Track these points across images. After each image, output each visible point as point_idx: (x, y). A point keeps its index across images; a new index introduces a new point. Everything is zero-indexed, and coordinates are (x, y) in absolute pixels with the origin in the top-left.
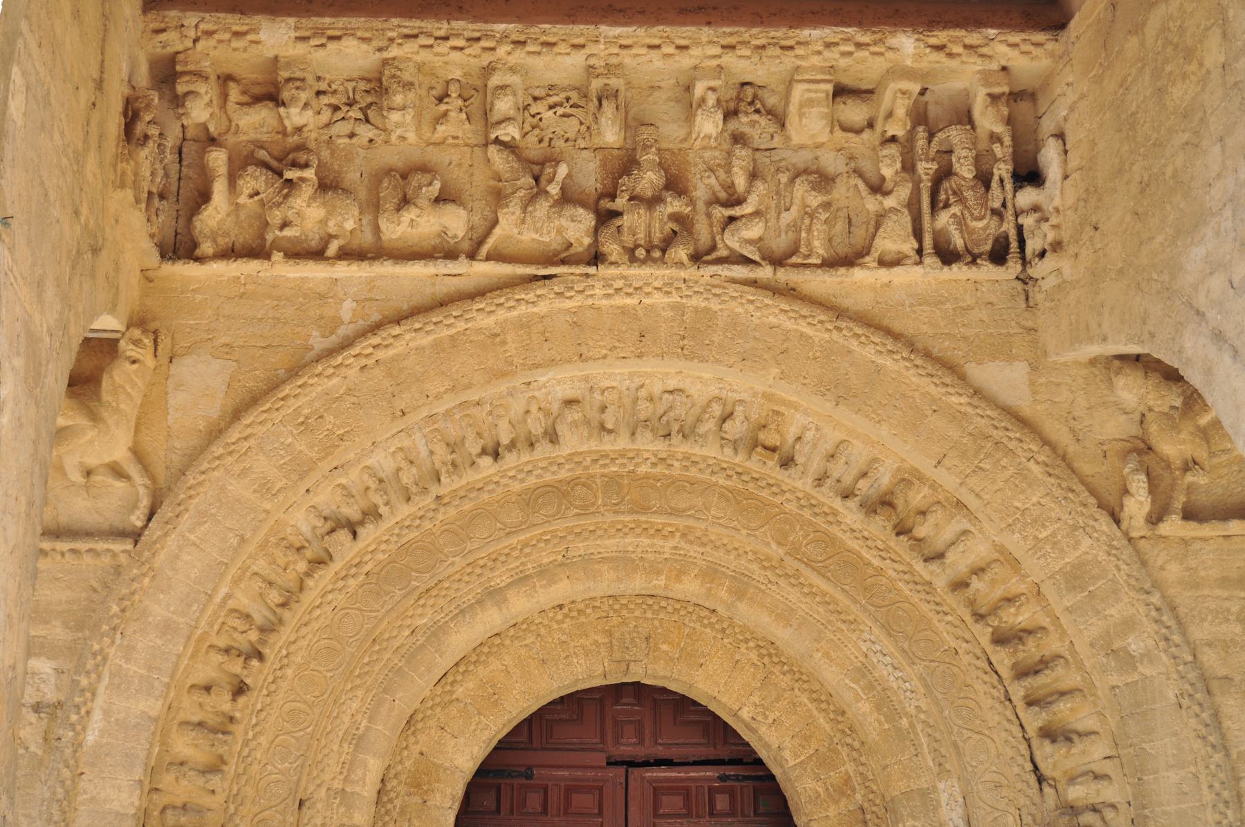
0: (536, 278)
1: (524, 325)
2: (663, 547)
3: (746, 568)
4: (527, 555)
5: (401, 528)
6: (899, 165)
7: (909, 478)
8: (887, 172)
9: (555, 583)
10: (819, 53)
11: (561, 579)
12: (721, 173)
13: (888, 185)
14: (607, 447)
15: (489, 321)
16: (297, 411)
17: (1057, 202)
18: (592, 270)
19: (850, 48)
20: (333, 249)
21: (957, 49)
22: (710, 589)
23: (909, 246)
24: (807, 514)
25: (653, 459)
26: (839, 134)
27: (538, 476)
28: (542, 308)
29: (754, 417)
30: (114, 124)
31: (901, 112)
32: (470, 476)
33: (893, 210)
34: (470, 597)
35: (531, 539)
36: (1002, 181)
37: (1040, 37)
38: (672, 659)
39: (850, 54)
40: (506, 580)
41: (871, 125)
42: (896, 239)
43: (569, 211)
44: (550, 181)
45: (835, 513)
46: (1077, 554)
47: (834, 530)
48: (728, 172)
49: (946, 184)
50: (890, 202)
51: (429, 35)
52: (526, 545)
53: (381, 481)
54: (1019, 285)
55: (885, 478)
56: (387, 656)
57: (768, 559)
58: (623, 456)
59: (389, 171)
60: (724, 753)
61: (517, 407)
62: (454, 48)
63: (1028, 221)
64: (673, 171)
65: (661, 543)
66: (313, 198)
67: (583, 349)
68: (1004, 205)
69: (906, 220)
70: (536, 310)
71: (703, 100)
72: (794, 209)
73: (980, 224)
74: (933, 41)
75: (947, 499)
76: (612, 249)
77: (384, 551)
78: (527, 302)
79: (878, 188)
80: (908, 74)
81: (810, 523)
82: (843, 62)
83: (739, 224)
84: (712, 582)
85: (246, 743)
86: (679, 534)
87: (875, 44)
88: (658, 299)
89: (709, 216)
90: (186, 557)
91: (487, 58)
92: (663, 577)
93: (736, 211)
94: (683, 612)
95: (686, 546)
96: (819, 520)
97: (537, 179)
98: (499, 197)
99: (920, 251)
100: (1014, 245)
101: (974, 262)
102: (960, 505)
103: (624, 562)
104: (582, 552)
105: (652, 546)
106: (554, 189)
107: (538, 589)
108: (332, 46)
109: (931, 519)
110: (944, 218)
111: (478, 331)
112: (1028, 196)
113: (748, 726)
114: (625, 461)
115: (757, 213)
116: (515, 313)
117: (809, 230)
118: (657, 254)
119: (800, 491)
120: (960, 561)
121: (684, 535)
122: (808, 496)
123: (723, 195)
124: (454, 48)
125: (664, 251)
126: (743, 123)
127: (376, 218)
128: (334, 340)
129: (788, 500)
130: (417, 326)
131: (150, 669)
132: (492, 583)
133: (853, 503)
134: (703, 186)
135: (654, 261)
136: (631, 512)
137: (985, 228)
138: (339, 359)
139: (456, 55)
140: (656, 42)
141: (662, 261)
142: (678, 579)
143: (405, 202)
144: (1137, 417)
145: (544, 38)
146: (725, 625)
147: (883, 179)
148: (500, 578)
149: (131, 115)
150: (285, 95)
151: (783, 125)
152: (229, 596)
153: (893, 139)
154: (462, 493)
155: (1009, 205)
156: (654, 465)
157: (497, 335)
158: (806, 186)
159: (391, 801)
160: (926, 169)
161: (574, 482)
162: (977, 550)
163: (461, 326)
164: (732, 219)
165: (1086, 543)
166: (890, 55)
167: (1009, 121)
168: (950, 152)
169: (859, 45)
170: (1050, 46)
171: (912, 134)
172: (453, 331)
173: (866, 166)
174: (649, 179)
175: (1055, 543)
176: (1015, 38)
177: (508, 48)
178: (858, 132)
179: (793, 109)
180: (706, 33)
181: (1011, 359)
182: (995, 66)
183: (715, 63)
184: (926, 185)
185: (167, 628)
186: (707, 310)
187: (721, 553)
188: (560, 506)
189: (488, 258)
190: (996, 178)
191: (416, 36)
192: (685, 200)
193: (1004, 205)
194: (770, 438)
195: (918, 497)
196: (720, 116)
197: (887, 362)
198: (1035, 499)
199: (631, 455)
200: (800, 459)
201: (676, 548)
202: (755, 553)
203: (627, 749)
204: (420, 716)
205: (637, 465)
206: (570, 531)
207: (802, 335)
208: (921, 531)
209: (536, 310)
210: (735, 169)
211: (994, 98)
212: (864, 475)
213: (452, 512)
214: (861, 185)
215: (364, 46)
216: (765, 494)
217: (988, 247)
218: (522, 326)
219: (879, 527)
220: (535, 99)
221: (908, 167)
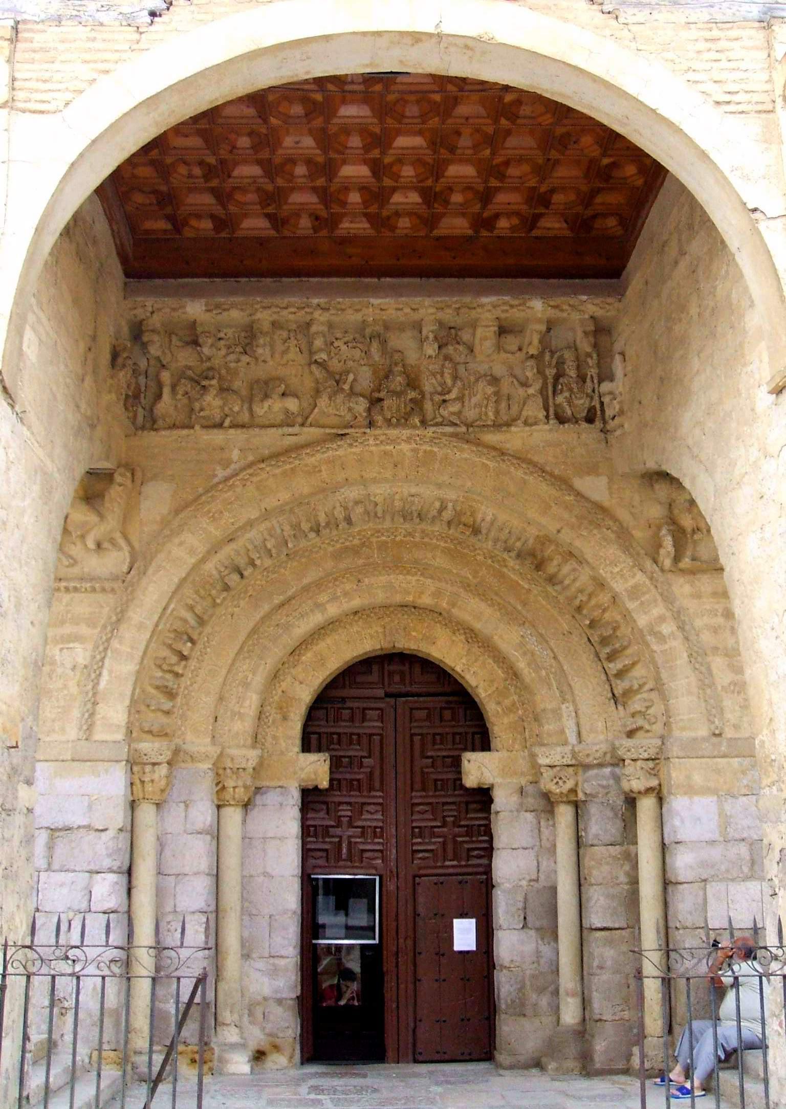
0: (339, 435)
1: (330, 462)
5: (268, 572)
6: (535, 370)
7: (544, 540)
8: (529, 374)
10: (489, 311)
12: (438, 376)
13: (530, 382)
16: (209, 512)
17: (621, 389)
18: (368, 431)
19: (505, 308)
20: (227, 423)
21: (565, 307)
23: (541, 414)
29: (458, 508)
30: (106, 357)
31: (536, 341)
33: (534, 395)
36: (592, 377)
37: (610, 300)
39: (507, 311)
41: (520, 349)
42: (534, 410)
43: (353, 399)
44: (344, 383)
45: (504, 560)
47: (505, 570)
48: (442, 376)
49: (561, 380)
50: (531, 391)
51: (277, 306)
53: (255, 547)
54: (603, 435)
59: (257, 381)
60: (448, 689)
62: (291, 313)
63: (606, 400)
64: (413, 376)
66: (216, 396)
68: (594, 391)
69: (540, 400)
71: (427, 338)
72: (478, 396)
73: (582, 401)
74: (552, 303)
76: (379, 419)
78: (332, 449)
79: (525, 384)
80: (539, 321)
82: (503, 316)
83: (448, 404)
85: (186, 688)
87: (520, 305)
88: (405, 447)
89: (432, 400)
90: (151, 589)
91: (308, 318)
93: (447, 397)
97: (338, 382)
98: (317, 392)
99: (547, 417)
100: (599, 413)
101: (577, 422)
108: (225, 314)
110: (560, 399)
111: (306, 465)
112: (606, 387)
113: (460, 675)
115: (457, 399)
117: (486, 407)
123: (439, 389)
124: (291, 313)
125: (406, 420)
126: (450, 349)
127: (250, 405)
128: (229, 472)
130: (273, 463)
131: (132, 648)
134: (429, 384)
137: (582, 403)
138: (231, 482)
139: (291, 317)
143: (266, 396)
145: (339, 306)
147: (527, 378)
149: (115, 355)
150: (201, 341)
151: (472, 351)
152: (173, 610)
153: (532, 356)
155: (596, 392)
157: (316, 467)
158: (485, 383)
159: (267, 717)
160: (551, 372)
163: (297, 462)
164: (444, 401)
166: (528, 311)
167: (595, 346)
168: (563, 363)
169: (512, 306)
170: (616, 305)
171: (542, 353)
172: (292, 466)
173: (518, 371)
174: (398, 381)
176: (597, 301)
177: (320, 312)
179: (477, 341)
180: (428, 301)
181: (598, 475)
182: (587, 316)
184: (550, 380)
185: (141, 626)
186: (431, 451)
189: (311, 425)
190: (589, 376)
191: (269, 307)
192: (417, 391)
193: (594, 391)
196: (436, 346)
197: (530, 479)
200: (484, 531)
203: (395, 688)
204: (281, 672)
207: (483, 463)
210: (446, 375)
211: (586, 333)
212: (519, 539)
214: (516, 382)
215: (242, 313)
217: (584, 414)
220: (337, 339)
221: (541, 372)
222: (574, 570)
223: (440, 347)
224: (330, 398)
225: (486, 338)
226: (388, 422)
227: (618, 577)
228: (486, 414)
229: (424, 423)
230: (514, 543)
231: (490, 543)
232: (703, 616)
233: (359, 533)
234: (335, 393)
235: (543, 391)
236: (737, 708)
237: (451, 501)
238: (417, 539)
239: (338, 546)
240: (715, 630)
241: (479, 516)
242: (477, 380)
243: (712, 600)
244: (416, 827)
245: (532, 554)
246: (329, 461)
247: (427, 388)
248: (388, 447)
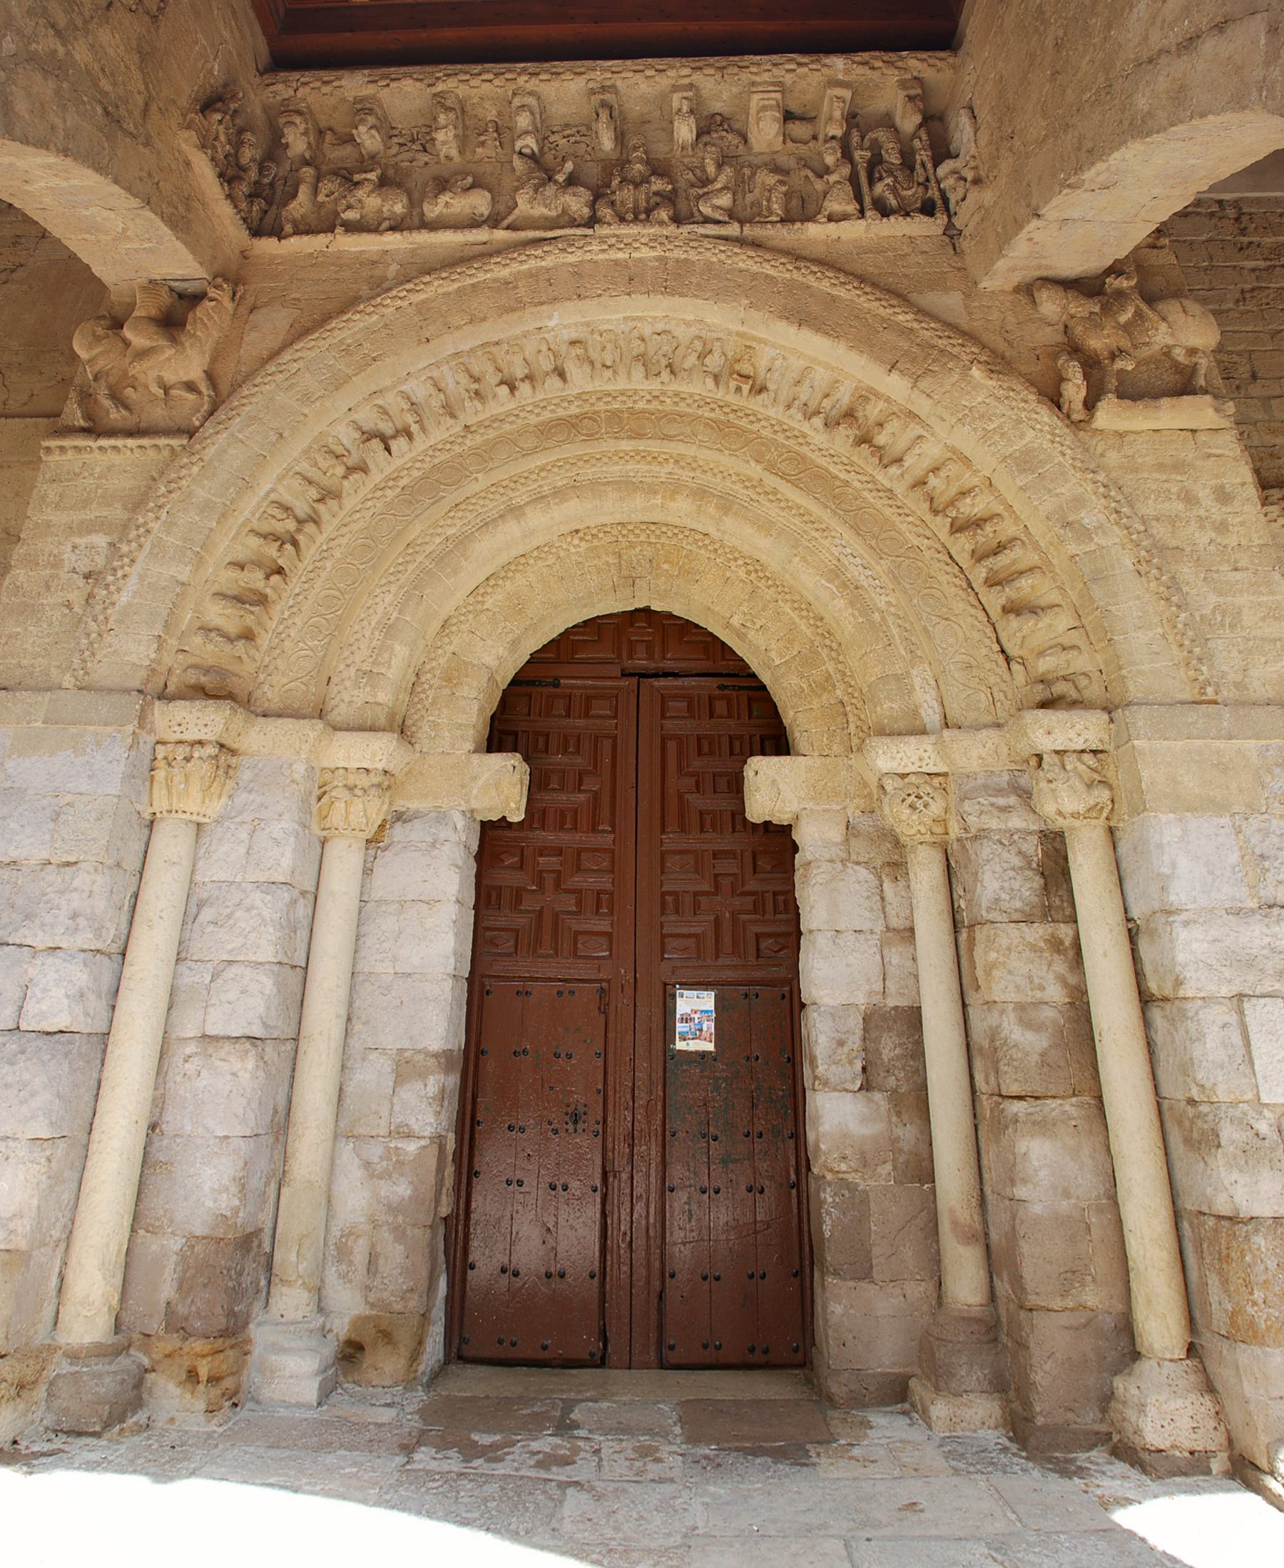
4: (543, 478)
14: (609, 387)
15: (505, 273)
22: (700, 506)
24: (780, 438)
25: (648, 397)
26: (789, 144)
27: (552, 411)
28: (549, 262)
32: (494, 409)
38: (672, 576)
40: (526, 498)
43: (571, 190)
46: (1024, 442)
47: (805, 450)
52: (542, 469)
55: (844, 396)
56: (420, 558)
57: (750, 480)
58: (622, 394)
61: (530, 348)
65: (658, 469)
67: (581, 291)
70: (543, 263)
75: (901, 411)
77: (418, 469)
81: (783, 445)
88: (645, 253)
94: (681, 536)
95: (680, 472)
96: (791, 442)
102: (912, 415)
103: (627, 486)
106: (560, 178)
109: (888, 428)
114: (625, 398)
116: (525, 267)
118: (643, 216)
120: (916, 463)
121: (677, 462)
122: (780, 423)
129: (764, 427)
133: (818, 422)
135: (641, 221)
136: (630, 438)
140: (641, 68)
141: (647, 219)
142: (672, 498)
144: (1061, 327)
146: (717, 546)
148: (520, 497)
154: (487, 423)
156: (649, 401)
161: (581, 417)
162: (931, 451)
165: (1030, 434)
175: (1003, 434)
178: (806, 143)
183: (686, 81)
187: (709, 476)
194: (746, 368)
195: (873, 411)
198: (980, 399)
199: (630, 393)
200: (772, 387)
202: (738, 475)
205: (635, 402)
206: (580, 458)
208: (881, 439)
209: (543, 263)
212: (827, 396)
213: (478, 439)
216: (743, 423)
218: (532, 276)
219: (842, 438)
222: (920, 437)
223: (698, 136)
224: (536, 191)
225: (765, 108)
226: (622, 220)
227: (997, 437)
228: (769, 208)
229: (677, 220)
230: (820, 403)
231: (781, 409)
232: (1147, 498)
233: (578, 396)
234: (543, 184)
235: (853, 180)
236: (1234, 653)
237: (718, 339)
238: (668, 408)
239: (547, 415)
240: (1173, 520)
241: (763, 364)
242: (754, 174)
243: (1157, 476)
244: (669, 893)
245: (849, 415)
246: (530, 274)
247: (682, 184)
248: (620, 255)
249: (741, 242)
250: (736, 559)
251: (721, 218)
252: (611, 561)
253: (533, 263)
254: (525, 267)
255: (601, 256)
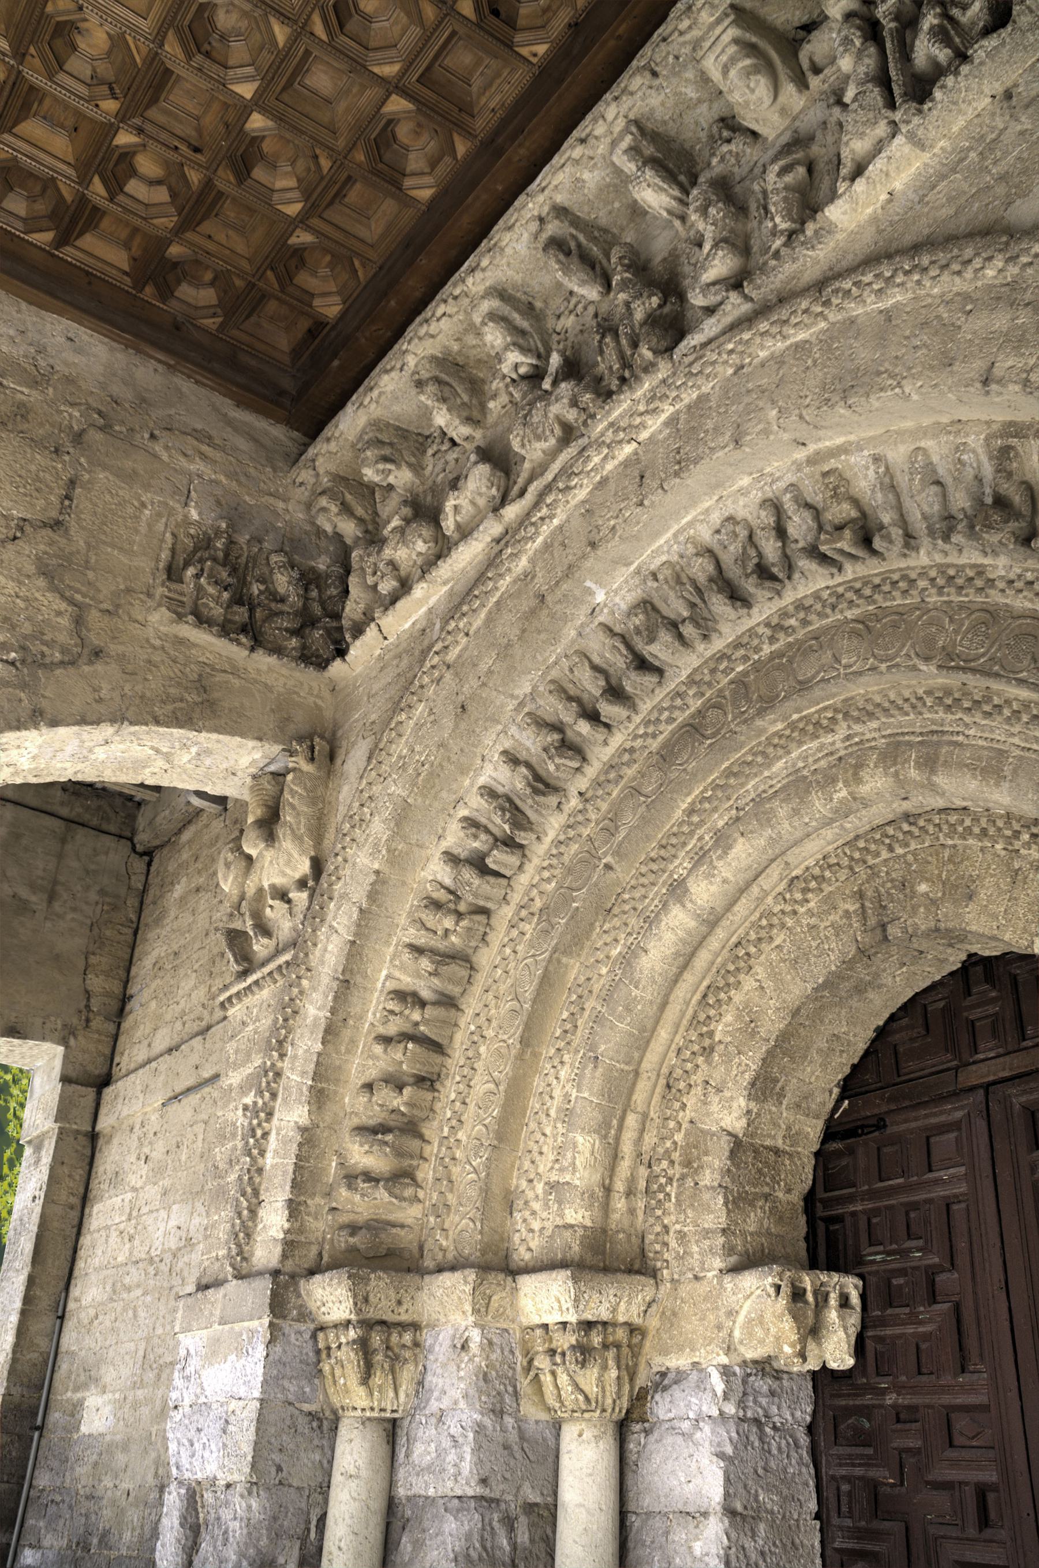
2: (833, 743)
3: (934, 722)
9: (730, 847)
11: (735, 841)
34: (656, 902)
35: (693, 803)
45: (980, 571)
47: (995, 597)
65: (829, 739)
70: (556, 522)
81: (962, 606)
84: (895, 764)
86: (840, 716)
92: (840, 785)
104: (753, 795)
105: (820, 749)
107: (715, 863)
114: (742, 652)
119: (931, 567)
121: (846, 715)
122: (942, 569)
132: (676, 877)
142: (859, 781)
188: (693, 747)
201: (848, 738)
209: (556, 522)
249: (763, 311)
250: (1017, 834)
251: (719, 298)
252: (852, 909)
253: (545, 529)
254: (540, 540)
255: (609, 466)
